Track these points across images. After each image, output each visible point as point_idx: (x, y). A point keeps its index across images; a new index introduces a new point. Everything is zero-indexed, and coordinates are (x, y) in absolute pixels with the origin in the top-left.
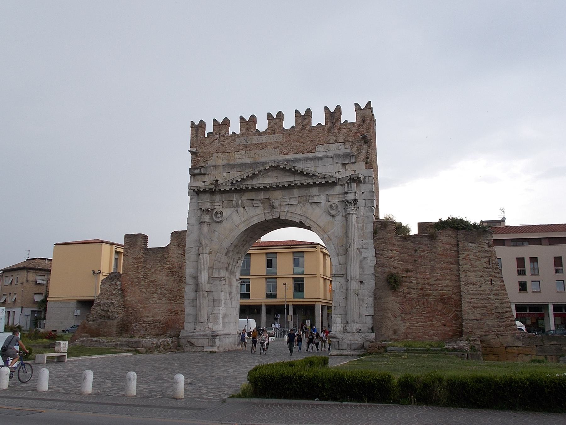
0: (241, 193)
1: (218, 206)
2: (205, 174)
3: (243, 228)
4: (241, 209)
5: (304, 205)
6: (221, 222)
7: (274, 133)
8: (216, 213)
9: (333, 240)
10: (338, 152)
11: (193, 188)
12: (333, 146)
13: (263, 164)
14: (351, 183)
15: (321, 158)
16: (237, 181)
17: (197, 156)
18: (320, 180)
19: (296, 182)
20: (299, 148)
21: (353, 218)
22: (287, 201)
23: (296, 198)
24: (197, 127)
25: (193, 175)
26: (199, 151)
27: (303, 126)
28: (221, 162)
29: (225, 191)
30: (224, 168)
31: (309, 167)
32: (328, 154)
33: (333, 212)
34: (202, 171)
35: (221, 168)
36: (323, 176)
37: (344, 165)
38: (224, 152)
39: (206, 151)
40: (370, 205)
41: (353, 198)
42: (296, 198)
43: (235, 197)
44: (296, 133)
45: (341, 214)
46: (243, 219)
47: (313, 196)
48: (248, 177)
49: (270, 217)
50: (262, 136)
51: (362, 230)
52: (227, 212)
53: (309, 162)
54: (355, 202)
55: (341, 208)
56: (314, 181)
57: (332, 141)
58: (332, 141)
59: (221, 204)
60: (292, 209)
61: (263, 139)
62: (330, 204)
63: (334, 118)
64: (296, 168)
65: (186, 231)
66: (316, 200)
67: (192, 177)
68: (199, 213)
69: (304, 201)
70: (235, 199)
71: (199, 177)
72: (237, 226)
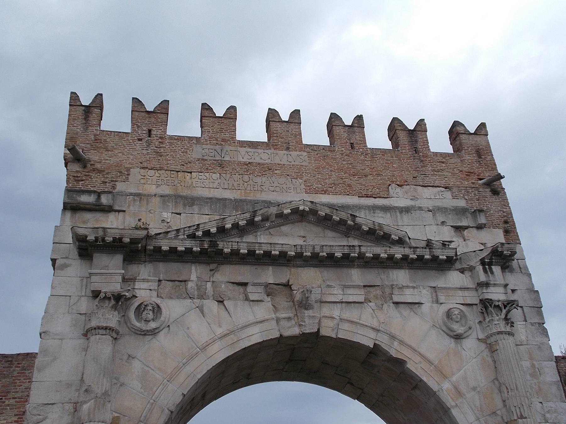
0: (213, 266)
1: (144, 292)
2: (108, 210)
3: (219, 353)
4: (211, 305)
5: (381, 308)
6: (154, 333)
7: (288, 149)
8: (140, 310)
9: (468, 396)
10: (439, 203)
11: (81, 231)
12: (428, 192)
13: (269, 204)
14: (490, 264)
15: (407, 210)
16: (207, 233)
17: (85, 167)
18: (419, 252)
19: (363, 249)
20: (349, 186)
21: (506, 344)
22: (337, 294)
23: (358, 287)
24: (88, 109)
25: (71, 207)
26: (92, 156)
27: (352, 144)
28: (152, 189)
29: (174, 256)
30: (164, 202)
31: (384, 220)
32: (418, 203)
33: (459, 329)
34: (105, 200)
35: (156, 201)
36: (424, 244)
37: (458, 229)
38: (161, 169)
39: (113, 161)
40: (536, 320)
41: (502, 297)
42: (358, 287)
43: (195, 273)
44: (338, 156)
45: (474, 335)
46: (219, 331)
47: (402, 288)
48: (236, 226)
49: (292, 330)
50: (260, 151)
51: (533, 375)
52: (173, 308)
53: (380, 214)
54: (510, 304)
55: (473, 316)
56: (407, 251)
57: (420, 181)
58: (420, 181)
59: (154, 285)
60: (351, 314)
61: (263, 157)
62: (443, 309)
63: (416, 141)
64: (358, 220)
65: (30, 357)
66: (409, 296)
67: (68, 214)
68: (85, 305)
69: (376, 297)
70: (193, 277)
71: (88, 216)
72: (204, 348)
